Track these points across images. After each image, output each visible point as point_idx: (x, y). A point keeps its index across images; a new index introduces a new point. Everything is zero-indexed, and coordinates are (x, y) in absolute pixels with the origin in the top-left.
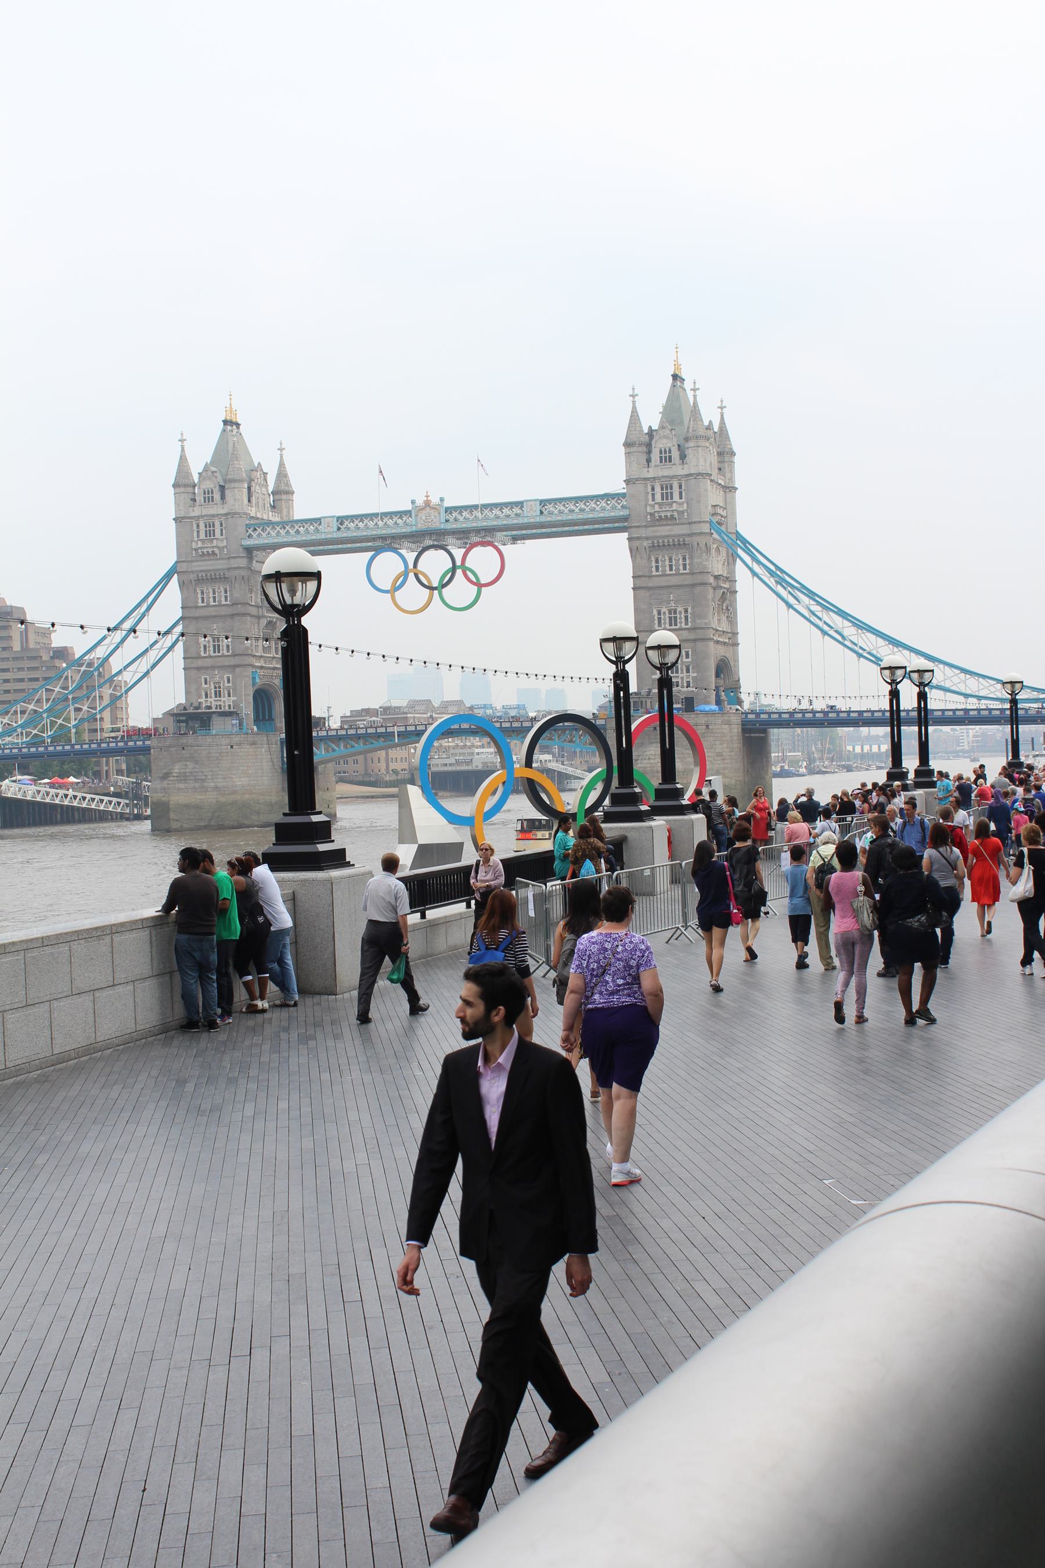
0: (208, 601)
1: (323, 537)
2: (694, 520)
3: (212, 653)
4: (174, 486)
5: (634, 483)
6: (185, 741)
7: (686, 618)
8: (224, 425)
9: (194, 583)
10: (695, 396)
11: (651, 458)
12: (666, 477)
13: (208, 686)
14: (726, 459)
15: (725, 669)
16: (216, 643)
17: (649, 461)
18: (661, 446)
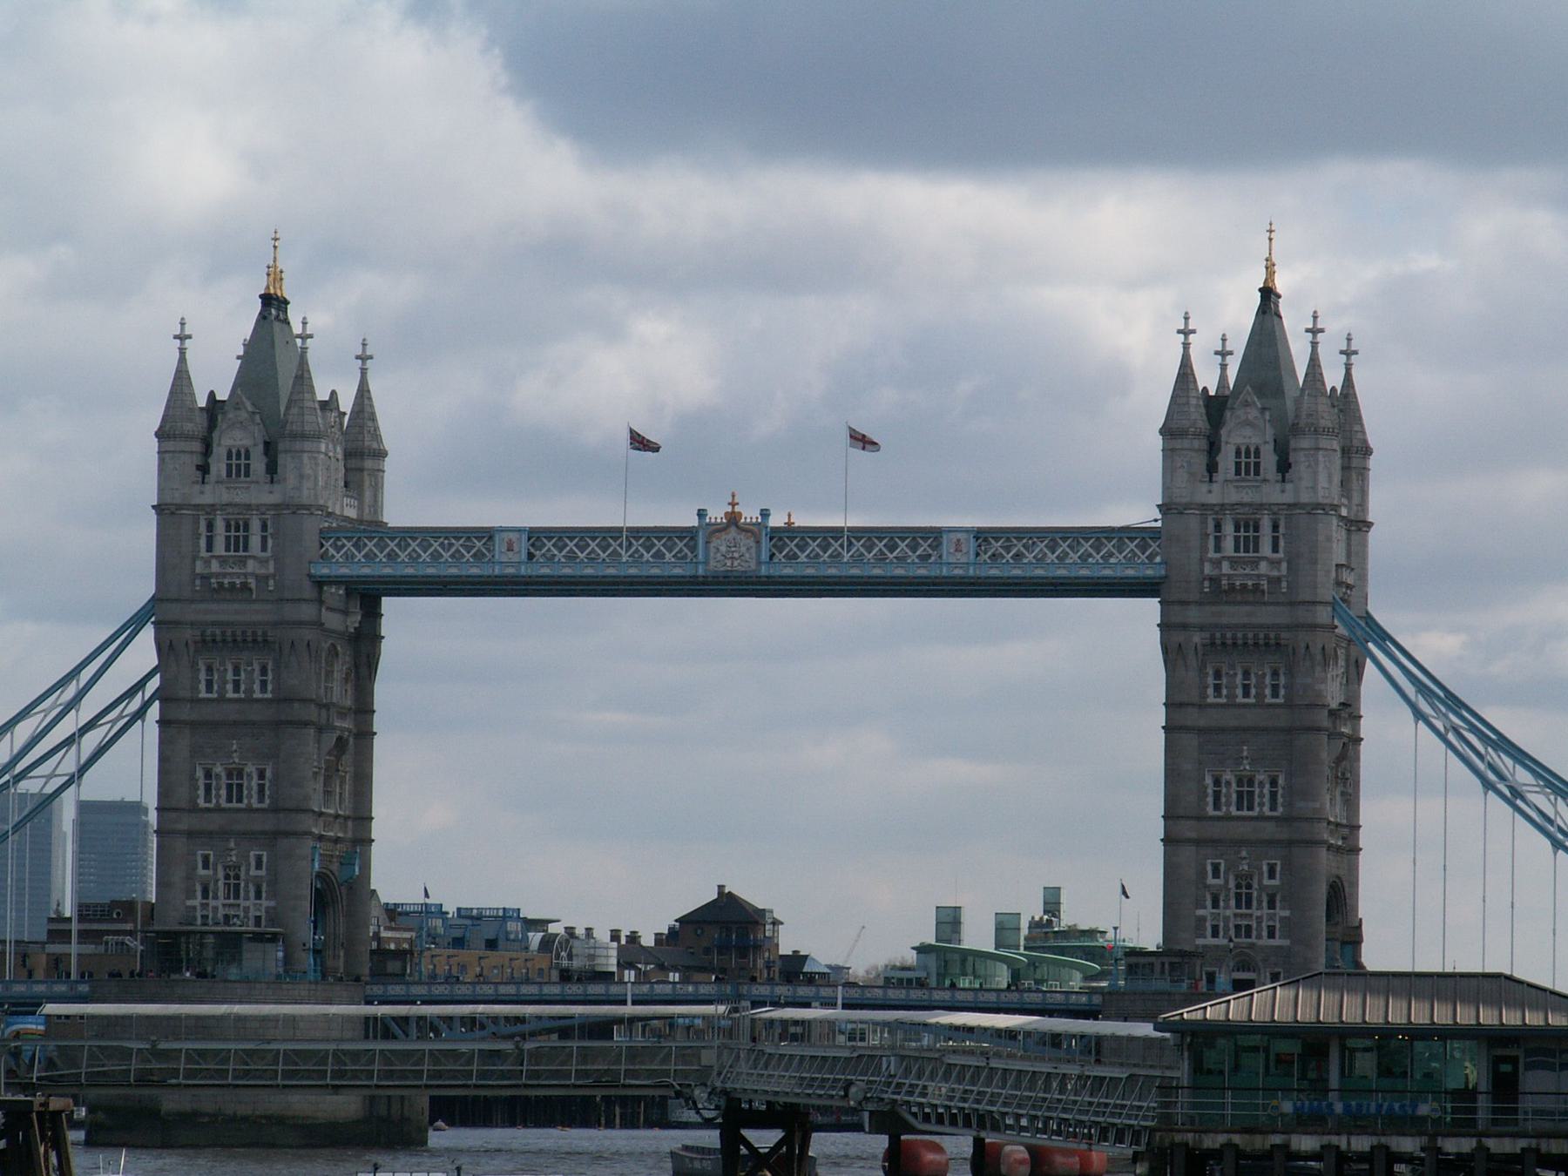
0: (222, 690)
1: (497, 572)
2: (1300, 598)
3: (224, 804)
4: (161, 435)
5: (1182, 513)
7: (1273, 795)
8: (264, 304)
9: (192, 649)
11: (1217, 464)
12: (1250, 505)
13: (210, 872)
14: (1355, 463)
15: (1340, 898)
17: (1212, 468)
18: (1239, 440)
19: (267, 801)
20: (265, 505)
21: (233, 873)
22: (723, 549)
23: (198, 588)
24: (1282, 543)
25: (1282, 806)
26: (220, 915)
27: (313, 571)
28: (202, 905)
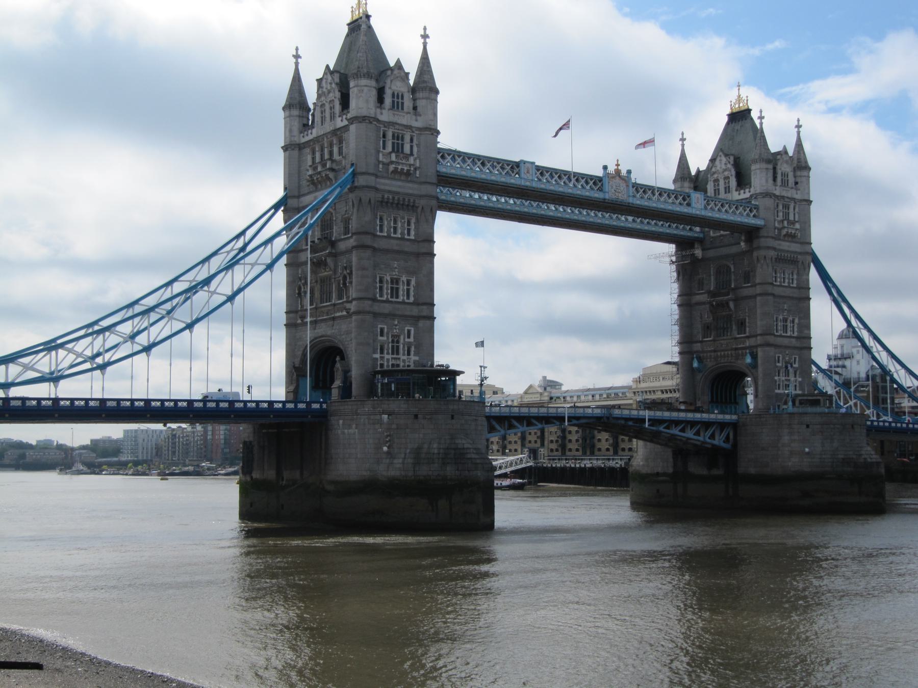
1: (523, 183)
2: (807, 241)
3: (390, 299)
5: (771, 197)
6: (456, 407)
7: (793, 326)
10: (799, 133)
13: (385, 338)
16: (395, 286)
17: (775, 179)
19: (412, 299)
20: (414, 127)
21: (396, 339)
22: (614, 187)
23: (380, 170)
24: (797, 216)
25: (797, 332)
26: (390, 363)
27: (438, 169)
28: (381, 357)
